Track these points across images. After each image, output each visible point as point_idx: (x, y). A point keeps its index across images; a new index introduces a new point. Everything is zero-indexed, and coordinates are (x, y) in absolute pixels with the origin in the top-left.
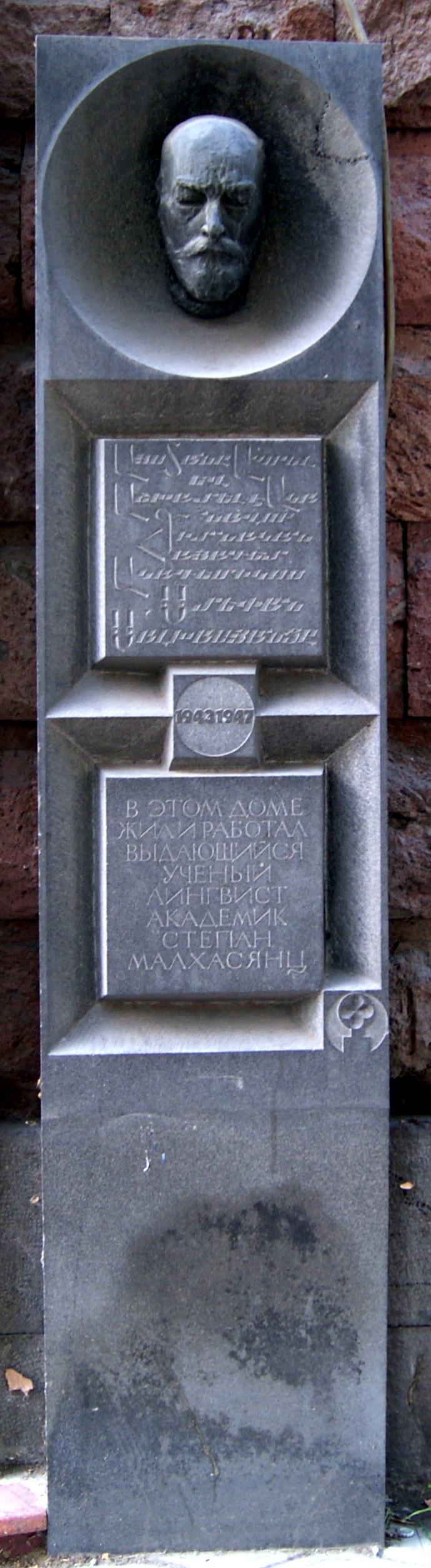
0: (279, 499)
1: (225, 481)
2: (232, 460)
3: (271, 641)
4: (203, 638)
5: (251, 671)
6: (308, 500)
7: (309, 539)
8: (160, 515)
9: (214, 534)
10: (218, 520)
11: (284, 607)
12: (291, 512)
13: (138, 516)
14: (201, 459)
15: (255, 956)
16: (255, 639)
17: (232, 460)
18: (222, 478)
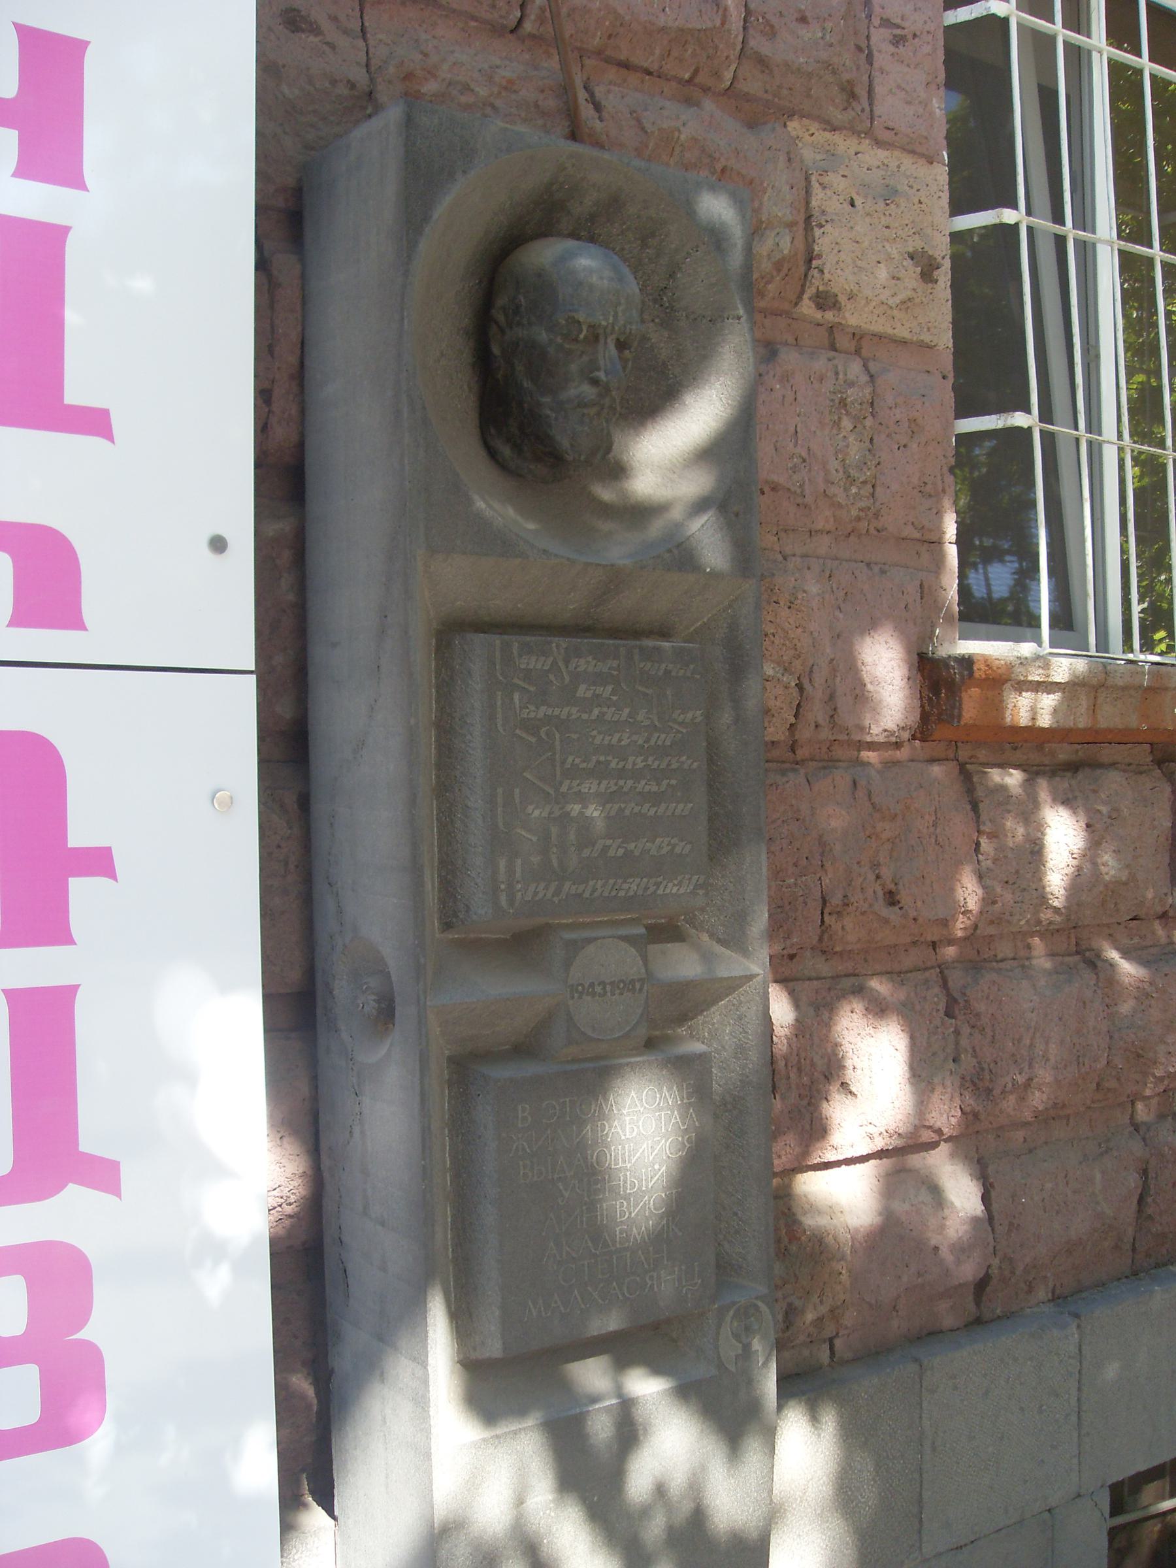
1: (614, 692)
3: (660, 892)
4: (594, 890)
5: (642, 930)
6: (694, 718)
7: (695, 764)
9: (602, 758)
11: (674, 846)
12: (678, 732)
13: (524, 735)
15: (651, 1278)
16: (646, 888)
18: (610, 688)
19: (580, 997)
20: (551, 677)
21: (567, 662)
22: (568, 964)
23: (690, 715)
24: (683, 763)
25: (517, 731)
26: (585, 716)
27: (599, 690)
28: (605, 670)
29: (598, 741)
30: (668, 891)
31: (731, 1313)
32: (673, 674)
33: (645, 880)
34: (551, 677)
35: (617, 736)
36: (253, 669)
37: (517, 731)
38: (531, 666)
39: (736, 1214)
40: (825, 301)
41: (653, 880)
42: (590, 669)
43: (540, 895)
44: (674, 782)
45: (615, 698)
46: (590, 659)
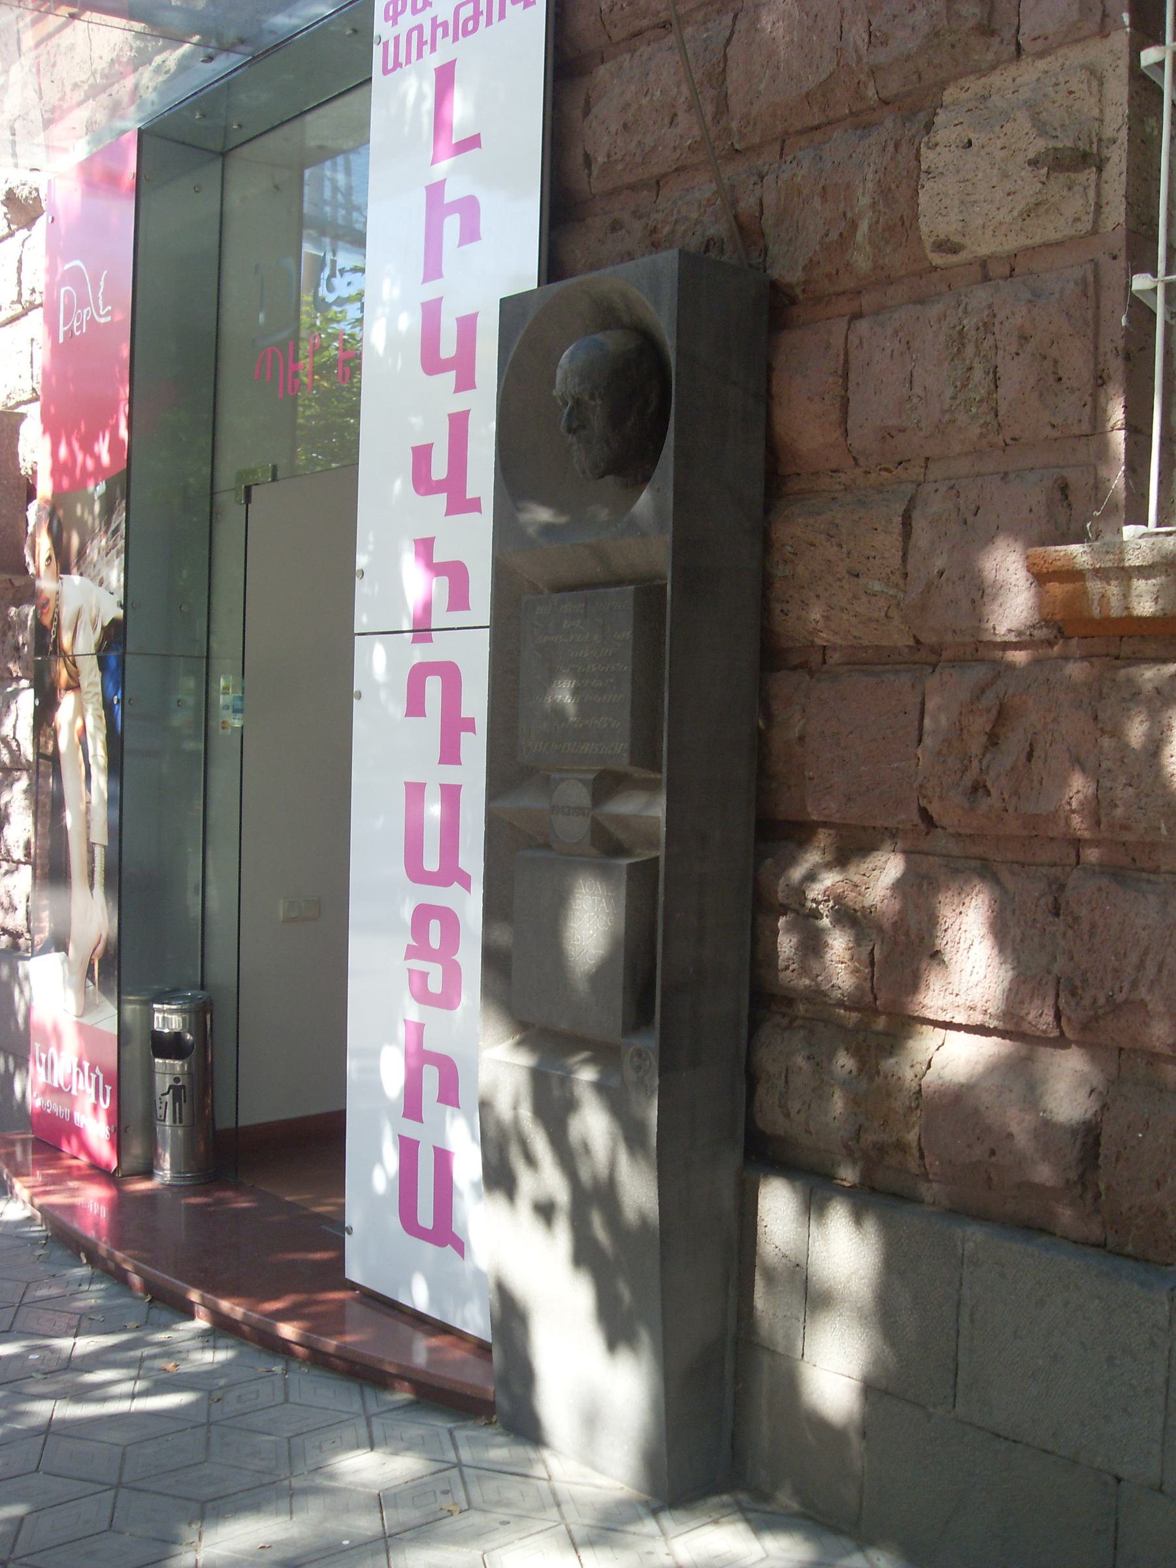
40: (946, 246)
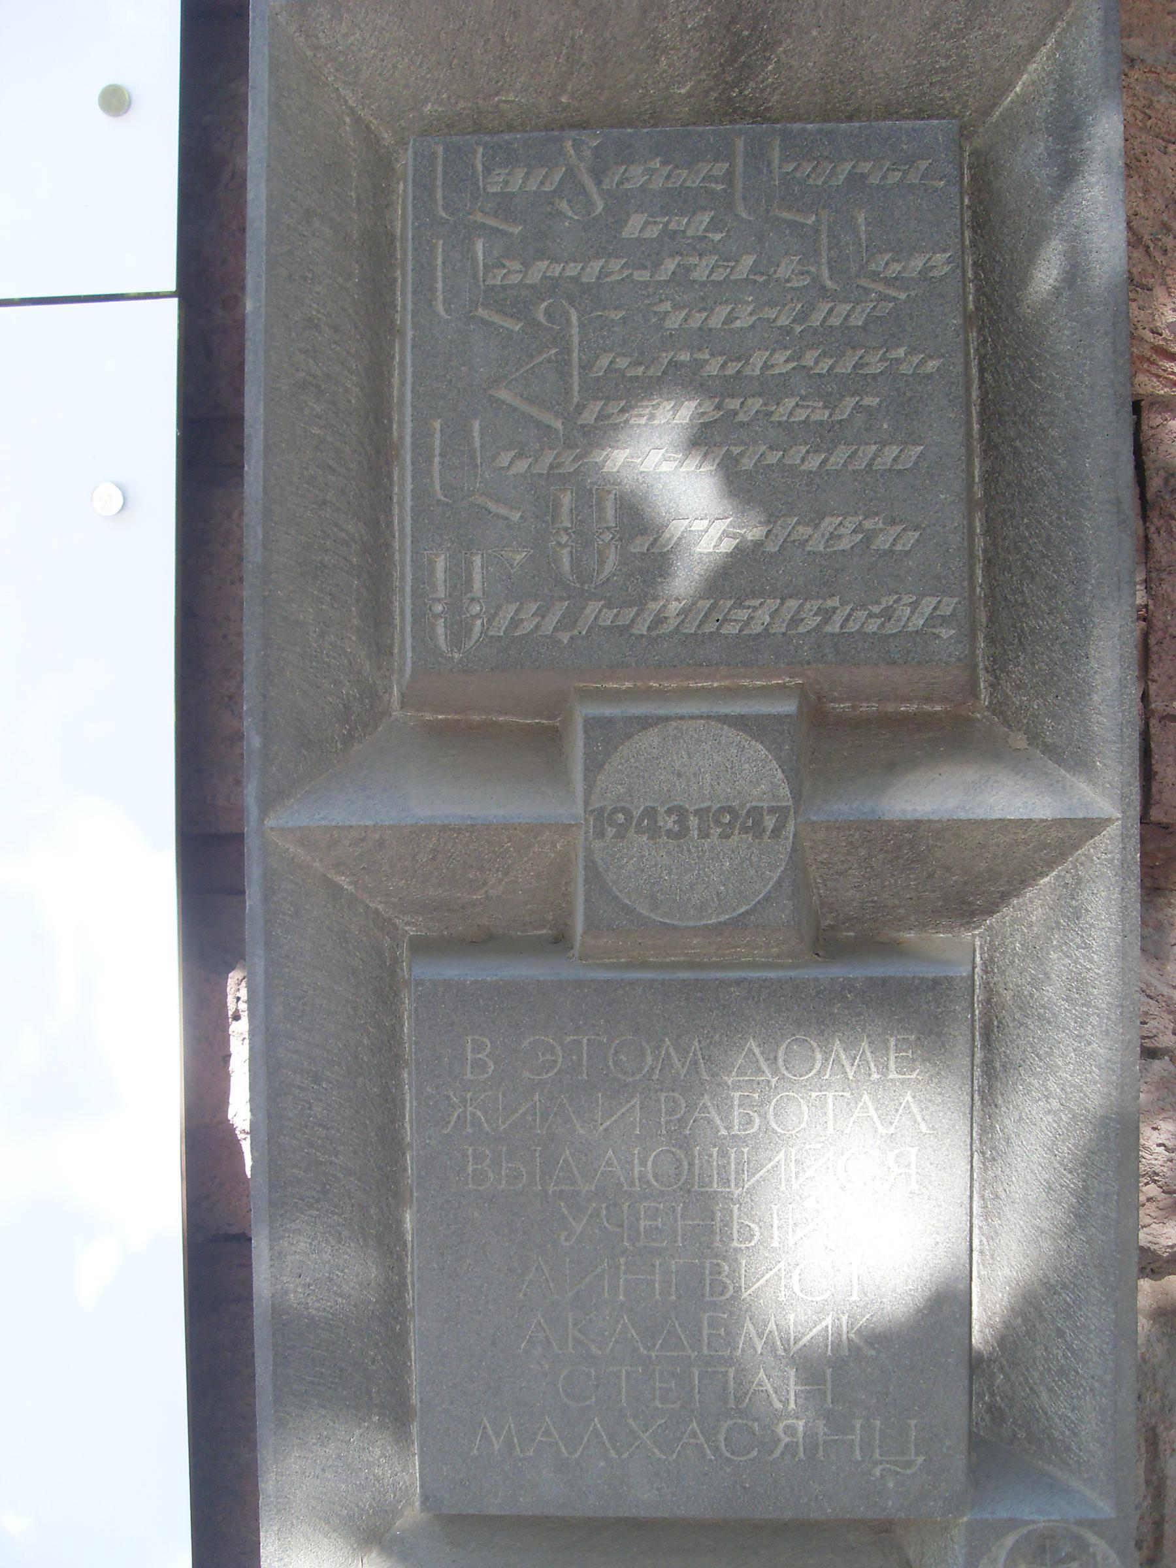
0: (854, 270)
1: (714, 225)
2: (730, 173)
3: (834, 628)
5: (788, 707)
7: (932, 365)
8: (547, 312)
9: (684, 357)
10: (695, 324)
13: (496, 319)
14: (652, 172)
16: (795, 621)
17: (730, 173)
18: (706, 218)
19: (621, 835)
20: (564, 206)
21: (598, 174)
22: (593, 767)
23: (918, 263)
24: (898, 361)
25: (481, 312)
26: (642, 276)
27: (678, 223)
28: (694, 182)
29: (674, 322)
30: (853, 627)
31: (1010, 1540)
32: (874, 180)
33: (793, 604)
34: (564, 206)
35: (722, 312)
36: (173, 287)
37: (481, 312)
38: (514, 188)
39: (1060, 1333)
41: (816, 604)
42: (658, 184)
43: (528, 626)
44: (871, 401)
45: (718, 237)
46: (656, 164)
